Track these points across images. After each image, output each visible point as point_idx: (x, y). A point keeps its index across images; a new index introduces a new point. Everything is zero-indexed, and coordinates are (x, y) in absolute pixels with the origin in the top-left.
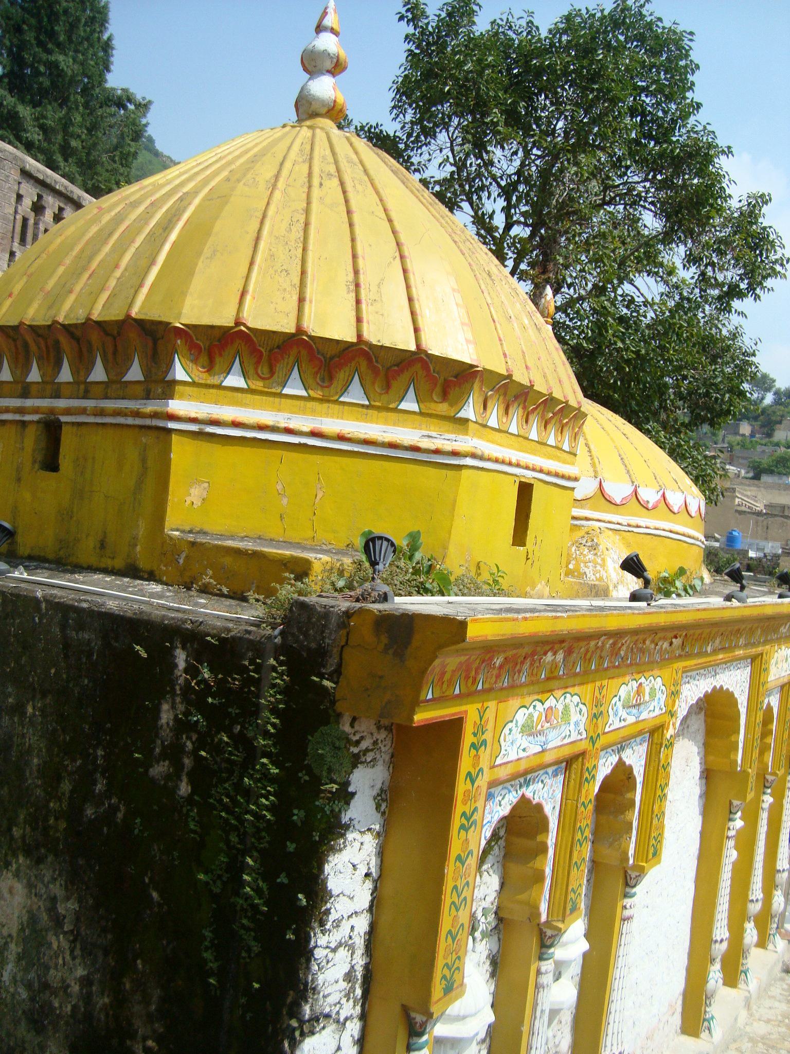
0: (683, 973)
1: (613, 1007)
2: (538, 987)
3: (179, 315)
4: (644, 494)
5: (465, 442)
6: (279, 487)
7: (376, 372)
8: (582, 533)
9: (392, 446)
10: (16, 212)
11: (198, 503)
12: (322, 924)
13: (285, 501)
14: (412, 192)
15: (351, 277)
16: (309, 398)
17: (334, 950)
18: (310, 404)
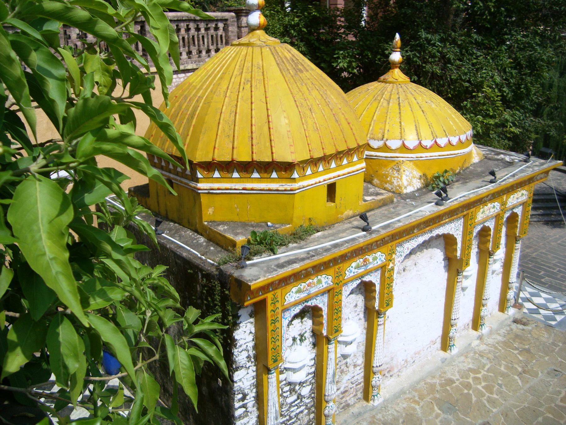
0: (441, 329)
2: (328, 352)
4: (424, 143)
5: (296, 185)
6: (236, 206)
7: (261, 168)
8: (395, 163)
9: (269, 190)
11: (211, 213)
12: (235, 347)
13: (238, 210)
14: (283, 75)
16: (241, 178)
17: (241, 352)
18: (242, 179)
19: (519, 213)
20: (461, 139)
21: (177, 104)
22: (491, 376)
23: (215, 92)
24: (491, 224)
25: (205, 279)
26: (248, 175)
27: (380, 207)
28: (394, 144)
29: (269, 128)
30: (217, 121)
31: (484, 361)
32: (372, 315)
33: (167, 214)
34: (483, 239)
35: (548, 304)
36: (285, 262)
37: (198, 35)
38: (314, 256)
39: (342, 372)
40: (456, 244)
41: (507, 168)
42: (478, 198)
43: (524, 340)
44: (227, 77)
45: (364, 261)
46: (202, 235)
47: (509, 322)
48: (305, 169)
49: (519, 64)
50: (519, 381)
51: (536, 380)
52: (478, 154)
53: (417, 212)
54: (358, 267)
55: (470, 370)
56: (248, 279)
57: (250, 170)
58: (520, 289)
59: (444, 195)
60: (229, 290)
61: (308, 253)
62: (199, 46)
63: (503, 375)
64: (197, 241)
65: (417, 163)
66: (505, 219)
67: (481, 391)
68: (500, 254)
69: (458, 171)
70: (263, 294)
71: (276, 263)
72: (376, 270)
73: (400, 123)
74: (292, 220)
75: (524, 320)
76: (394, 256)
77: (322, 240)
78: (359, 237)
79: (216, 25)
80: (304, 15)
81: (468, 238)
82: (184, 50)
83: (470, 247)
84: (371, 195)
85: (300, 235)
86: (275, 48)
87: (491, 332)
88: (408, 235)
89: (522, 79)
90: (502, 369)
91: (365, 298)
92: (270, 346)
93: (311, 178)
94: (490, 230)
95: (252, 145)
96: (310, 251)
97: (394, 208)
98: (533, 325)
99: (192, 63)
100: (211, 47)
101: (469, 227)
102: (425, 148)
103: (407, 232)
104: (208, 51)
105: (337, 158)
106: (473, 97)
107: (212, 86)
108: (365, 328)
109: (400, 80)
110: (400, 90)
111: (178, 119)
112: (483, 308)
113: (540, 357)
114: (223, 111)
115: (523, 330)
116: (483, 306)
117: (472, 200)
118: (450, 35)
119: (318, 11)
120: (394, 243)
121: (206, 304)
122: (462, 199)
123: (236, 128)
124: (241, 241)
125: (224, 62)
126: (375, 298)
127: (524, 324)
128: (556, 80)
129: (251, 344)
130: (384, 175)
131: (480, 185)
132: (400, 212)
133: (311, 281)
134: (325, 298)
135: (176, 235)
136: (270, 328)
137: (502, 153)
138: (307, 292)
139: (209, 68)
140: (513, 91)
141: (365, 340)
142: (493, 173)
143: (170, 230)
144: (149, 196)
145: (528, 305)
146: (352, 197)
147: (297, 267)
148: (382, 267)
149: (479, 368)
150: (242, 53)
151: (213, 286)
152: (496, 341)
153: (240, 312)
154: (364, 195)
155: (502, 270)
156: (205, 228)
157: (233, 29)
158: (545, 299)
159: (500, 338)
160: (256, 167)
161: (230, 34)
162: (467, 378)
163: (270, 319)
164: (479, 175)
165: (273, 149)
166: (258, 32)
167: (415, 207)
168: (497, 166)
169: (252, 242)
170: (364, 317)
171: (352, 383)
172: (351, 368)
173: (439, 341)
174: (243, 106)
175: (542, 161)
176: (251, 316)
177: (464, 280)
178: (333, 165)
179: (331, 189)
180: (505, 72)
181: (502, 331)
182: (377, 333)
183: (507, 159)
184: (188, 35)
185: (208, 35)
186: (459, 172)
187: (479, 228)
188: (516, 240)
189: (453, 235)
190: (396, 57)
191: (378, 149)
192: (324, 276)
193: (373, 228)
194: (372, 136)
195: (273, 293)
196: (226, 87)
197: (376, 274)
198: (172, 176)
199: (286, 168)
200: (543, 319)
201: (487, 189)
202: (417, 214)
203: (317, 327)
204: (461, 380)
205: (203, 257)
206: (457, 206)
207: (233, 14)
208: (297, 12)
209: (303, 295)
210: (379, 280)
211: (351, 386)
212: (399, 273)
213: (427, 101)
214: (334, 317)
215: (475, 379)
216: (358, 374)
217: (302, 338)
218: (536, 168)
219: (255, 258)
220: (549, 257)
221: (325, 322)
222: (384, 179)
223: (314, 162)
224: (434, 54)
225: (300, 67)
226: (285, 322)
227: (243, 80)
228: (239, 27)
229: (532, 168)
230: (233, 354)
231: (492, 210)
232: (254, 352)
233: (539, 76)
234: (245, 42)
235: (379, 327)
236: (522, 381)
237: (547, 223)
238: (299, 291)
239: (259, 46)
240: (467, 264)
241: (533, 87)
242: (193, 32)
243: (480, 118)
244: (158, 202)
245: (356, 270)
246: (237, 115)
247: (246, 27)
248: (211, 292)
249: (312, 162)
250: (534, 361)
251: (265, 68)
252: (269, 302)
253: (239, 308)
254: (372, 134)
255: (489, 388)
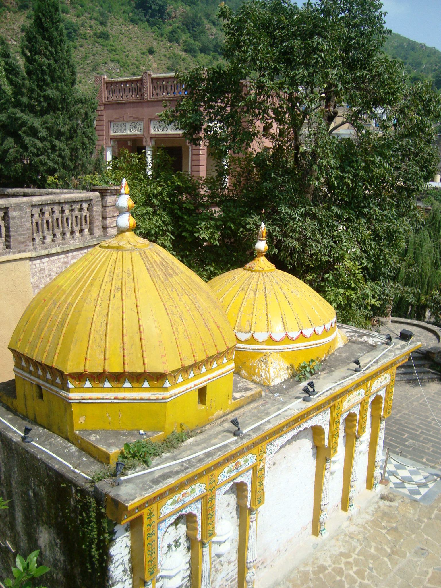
0: (312, 515)
1: (249, 548)
2: (203, 555)
3: (66, 369)
4: (290, 335)
5: (167, 394)
7: (133, 378)
10: (32, 223)
11: (83, 422)
12: (112, 562)
14: (153, 281)
15: (122, 345)
19: (383, 396)
20: (326, 328)
21: (46, 309)
22: (362, 560)
23: (85, 300)
24: (356, 410)
25: (79, 495)
26: (120, 385)
27: (249, 403)
28: (261, 336)
29: (141, 339)
30: (88, 332)
31: (354, 543)
32: (244, 512)
33: (35, 418)
34: (350, 424)
35: (413, 477)
36: (160, 477)
37: (62, 217)
38: (187, 468)
39: (217, 571)
40: (324, 433)
41: (370, 353)
42: (344, 390)
43: (391, 518)
44: (97, 283)
45: (236, 465)
46: (73, 443)
47: (377, 498)
48: (177, 377)
49: (378, 235)
50: (389, 563)
51: (404, 561)
52: (342, 338)
53: (286, 411)
54: (230, 471)
55: (342, 554)
56: (125, 498)
57: (122, 380)
58: (386, 462)
59: (311, 390)
60: (105, 507)
61: (181, 464)
62: (63, 228)
63: (373, 558)
64: (69, 451)
65: (284, 354)
66: (369, 403)
67: (353, 577)
68: (366, 436)
69: (323, 358)
70: (139, 511)
71: (151, 477)
72: (248, 471)
73: (267, 314)
74: (164, 427)
75: (391, 496)
76: (264, 455)
77: (194, 448)
78: (230, 443)
79: (81, 205)
80: (167, 184)
81: (335, 427)
82: (48, 234)
83: (337, 435)
84: (240, 391)
85: (172, 442)
86: (144, 252)
87: (359, 512)
88: (278, 433)
89: (381, 250)
90: (372, 550)
91: (237, 497)
92: (147, 559)
93: (182, 385)
94: (356, 415)
95: (124, 356)
96: (184, 462)
97: (263, 405)
98: (400, 501)
99: (56, 246)
100: (76, 229)
101: (336, 416)
102: (292, 339)
103: (278, 431)
104: (72, 232)
105: (207, 363)
106: (334, 269)
107: (82, 293)
108: (237, 525)
109: (266, 268)
110: (266, 279)
111: (48, 324)
112: (352, 489)
113: (407, 535)
114: (94, 321)
115: (390, 506)
116: (352, 487)
117: (338, 393)
118: (311, 210)
119: (181, 182)
120: (264, 443)
121: (80, 520)
122: (329, 393)
123: (108, 338)
124: (115, 453)
125: (94, 266)
126: (247, 497)
127: (391, 500)
128: (412, 236)
129: (128, 557)
130: (252, 366)
131: (345, 375)
132: (270, 410)
133: (185, 491)
134: (199, 505)
135: (46, 443)
136: (147, 542)
137: (366, 335)
138: (182, 502)
139: (78, 271)
140: (373, 261)
141: (238, 536)
142: (357, 362)
143: (40, 436)
144: (15, 397)
145: (393, 479)
146: (221, 398)
147: (171, 481)
148: (253, 468)
149: (350, 551)
150: (112, 258)
151: (87, 502)
152: (365, 520)
153: (116, 528)
154: (234, 391)
155: (368, 449)
156: (76, 437)
157: (97, 208)
158: (409, 471)
159: (369, 517)
160: (128, 377)
161: (94, 214)
162: (339, 564)
163: (146, 533)
164: (343, 362)
165: (145, 359)
166: (127, 234)
167: (284, 403)
168: (361, 350)
169: (126, 455)
170: (237, 514)
171: (227, 580)
172: (226, 566)
173: (310, 526)
174: (114, 316)
175: (403, 343)
176: (127, 530)
177: (332, 464)
178: (204, 370)
179: (202, 393)
180: (364, 244)
181: (371, 509)
182: (249, 529)
183: (371, 341)
184: (52, 218)
185: (72, 216)
186: (325, 360)
187: (345, 415)
188: (381, 420)
189: (320, 426)
190: (262, 245)
191: (246, 342)
192: (198, 485)
193: (244, 432)
194: (239, 328)
195: (149, 508)
196: (96, 295)
197: (248, 474)
198: (41, 382)
199: (158, 378)
200: (408, 493)
201: (352, 379)
202: (286, 413)
203: (191, 532)
204: (333, 566)
205: (77, 471)
206: (324, 401)
207: (97, 194)
208: (159, 182)
209: (177, 506)
210: (250, 480)
211: (225, 583)
212: (269, 467)
213: (293, 290)
214: (209, 522)
215: (347, 564)
216: (233, 570)
217: (177, 543)
218: (398, 352)
219: (130, 472)
220: (412, 418)
221: (199, 527)
222: (252, 371)
223: (185, 370)
224: (296, 228)
225: (170, 271)
226: (160, 533)
227: (113, 288)
228: (104, 207)
229: (394, 352)
230: (109, 570)
231: (357, 397)
232: (130, 565)
233: (396, 246)
234: (115, 245)
235: (252, 524)
236: (392, 564)
237: (409, 381)
238: (174, 503)
239: (128, 250)
240: (335, 452)
241: (391, 258)
242: (57, 214)
243: (342, 291)
244: (26, 405)
245: (229, 474)
246: (109, 324)
247: (111, 206)
248: (86, 507)
249: (183, 370)
250: (402, 540)
251: (135, 274)
252: (145, 517)
253: (115, 524)
254: (240, 326)
255: (360, 573)
